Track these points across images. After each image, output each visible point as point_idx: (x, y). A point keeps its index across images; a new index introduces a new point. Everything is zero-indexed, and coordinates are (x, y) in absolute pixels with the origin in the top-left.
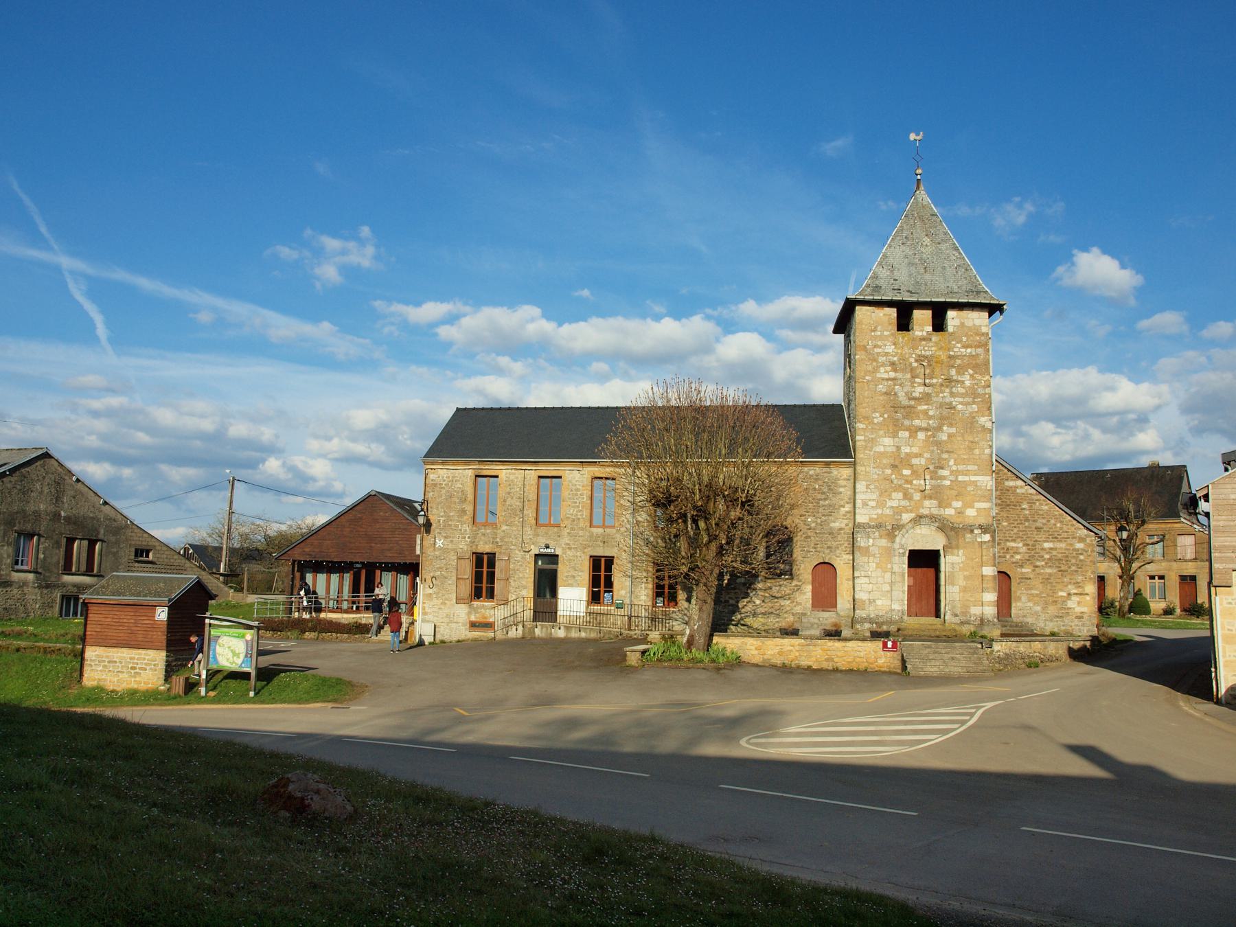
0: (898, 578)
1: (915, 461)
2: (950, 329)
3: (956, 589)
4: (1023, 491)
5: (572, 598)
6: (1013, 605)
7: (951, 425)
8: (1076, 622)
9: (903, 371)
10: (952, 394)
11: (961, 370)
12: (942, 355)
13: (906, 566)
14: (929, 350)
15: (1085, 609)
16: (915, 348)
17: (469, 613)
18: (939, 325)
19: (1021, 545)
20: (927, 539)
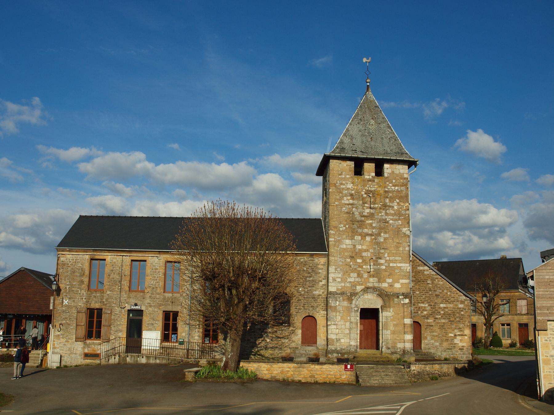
0: (354, 326)
1: (364, 254)
3: (389, 332)
4: (428, 273)
5: (151, 339)
6: (423, 342)
7: (385, 233)
8: (459, 352)
9: (358, 199)
10: (387, 214)
11: (392, 199)
13: (358, 318)
14: (373, 187)
15: (464, 344)
16: (365, 186)
17: (84, 348)
18: (379, 172)
19: (427, 305)
20: (371, 301)
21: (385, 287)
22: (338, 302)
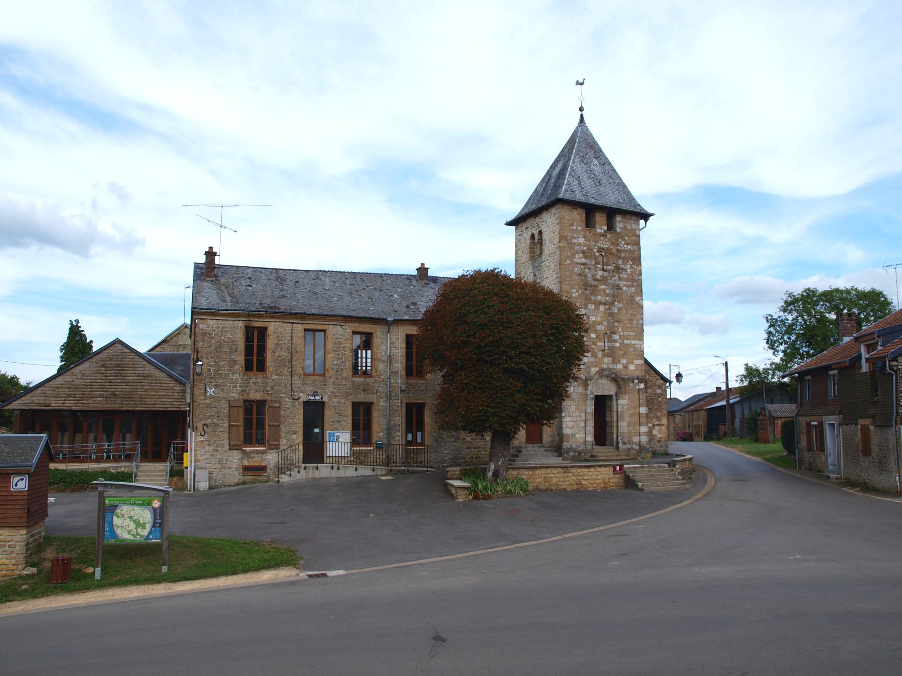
1: (598, 328)
2: (618, 230)
5: (339, 443)
7: (619, 302)
9: (590, 258)
10: (620, 278)
11: (625, 260)
12: (614, 249)
14: (605, 244)
15: (662, 435)
16: (596, 242)
17: (242, 459)
18: (611, 227)
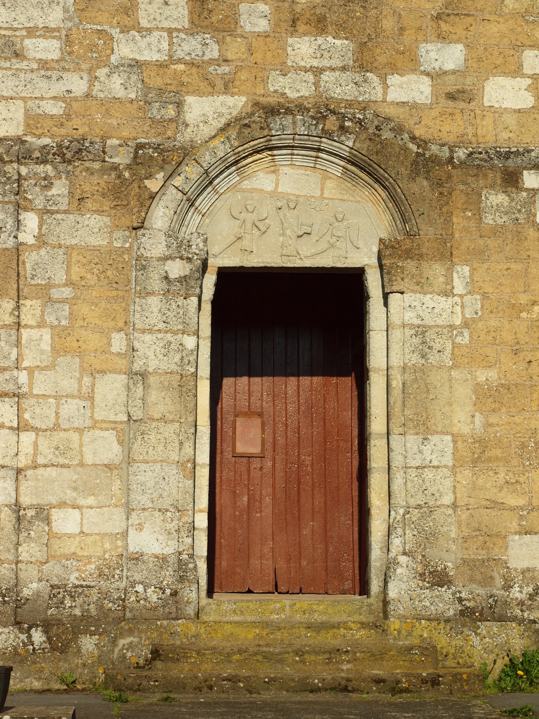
0: (161, 402)
21: (414, 106)
22: (30, 220)
